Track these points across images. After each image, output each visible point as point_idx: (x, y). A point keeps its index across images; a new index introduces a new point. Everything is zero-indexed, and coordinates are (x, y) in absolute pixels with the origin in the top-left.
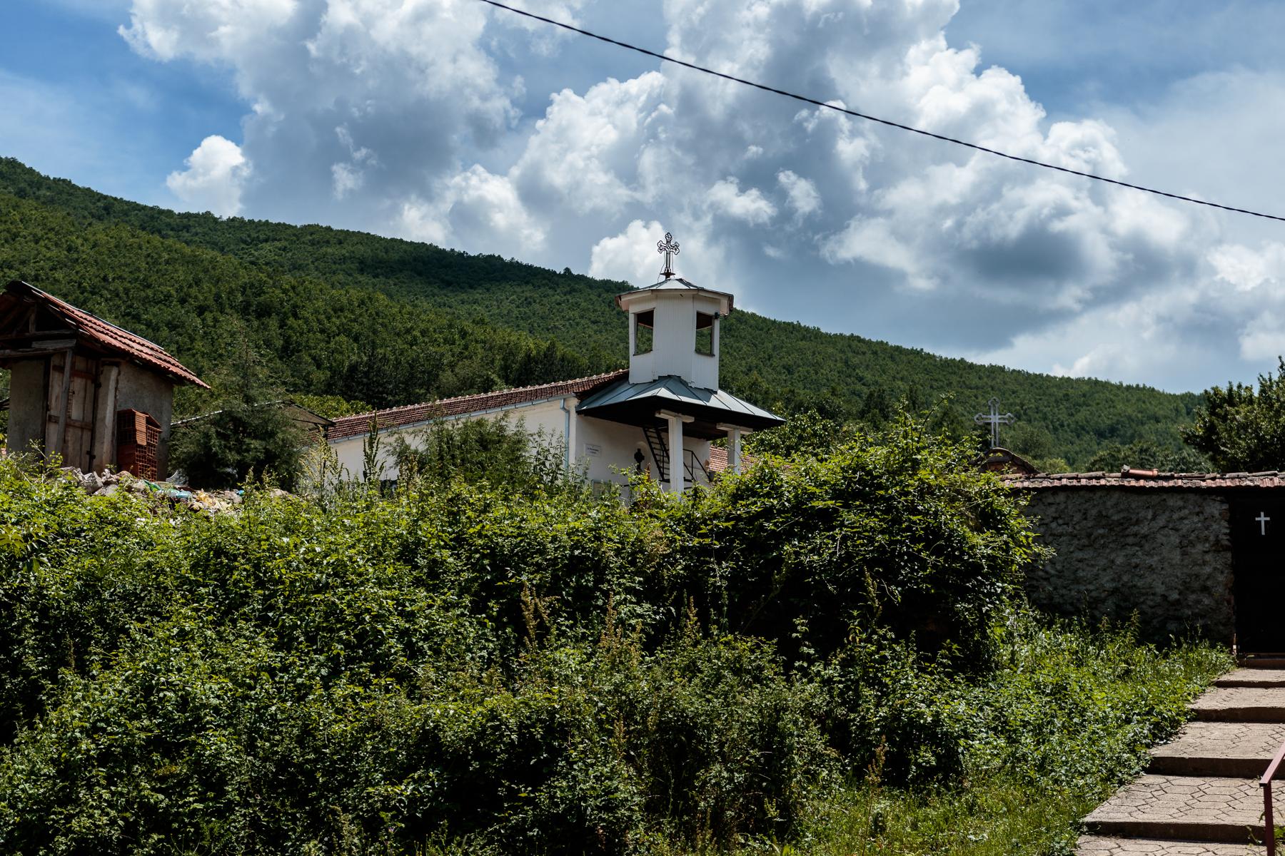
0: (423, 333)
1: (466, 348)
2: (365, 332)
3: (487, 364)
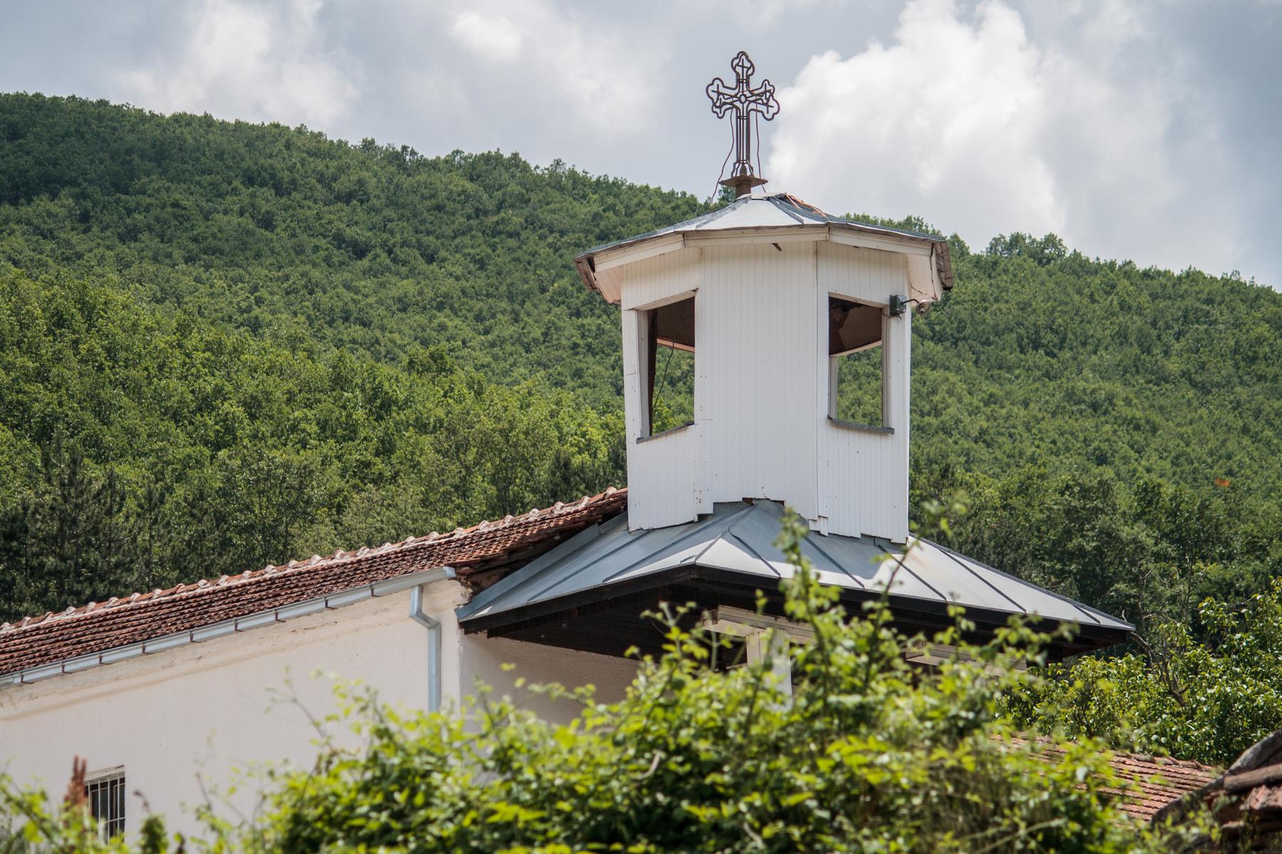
0: (253, 407)
1: (386, 449)
2: (72, 410)
3: (446, 497)
